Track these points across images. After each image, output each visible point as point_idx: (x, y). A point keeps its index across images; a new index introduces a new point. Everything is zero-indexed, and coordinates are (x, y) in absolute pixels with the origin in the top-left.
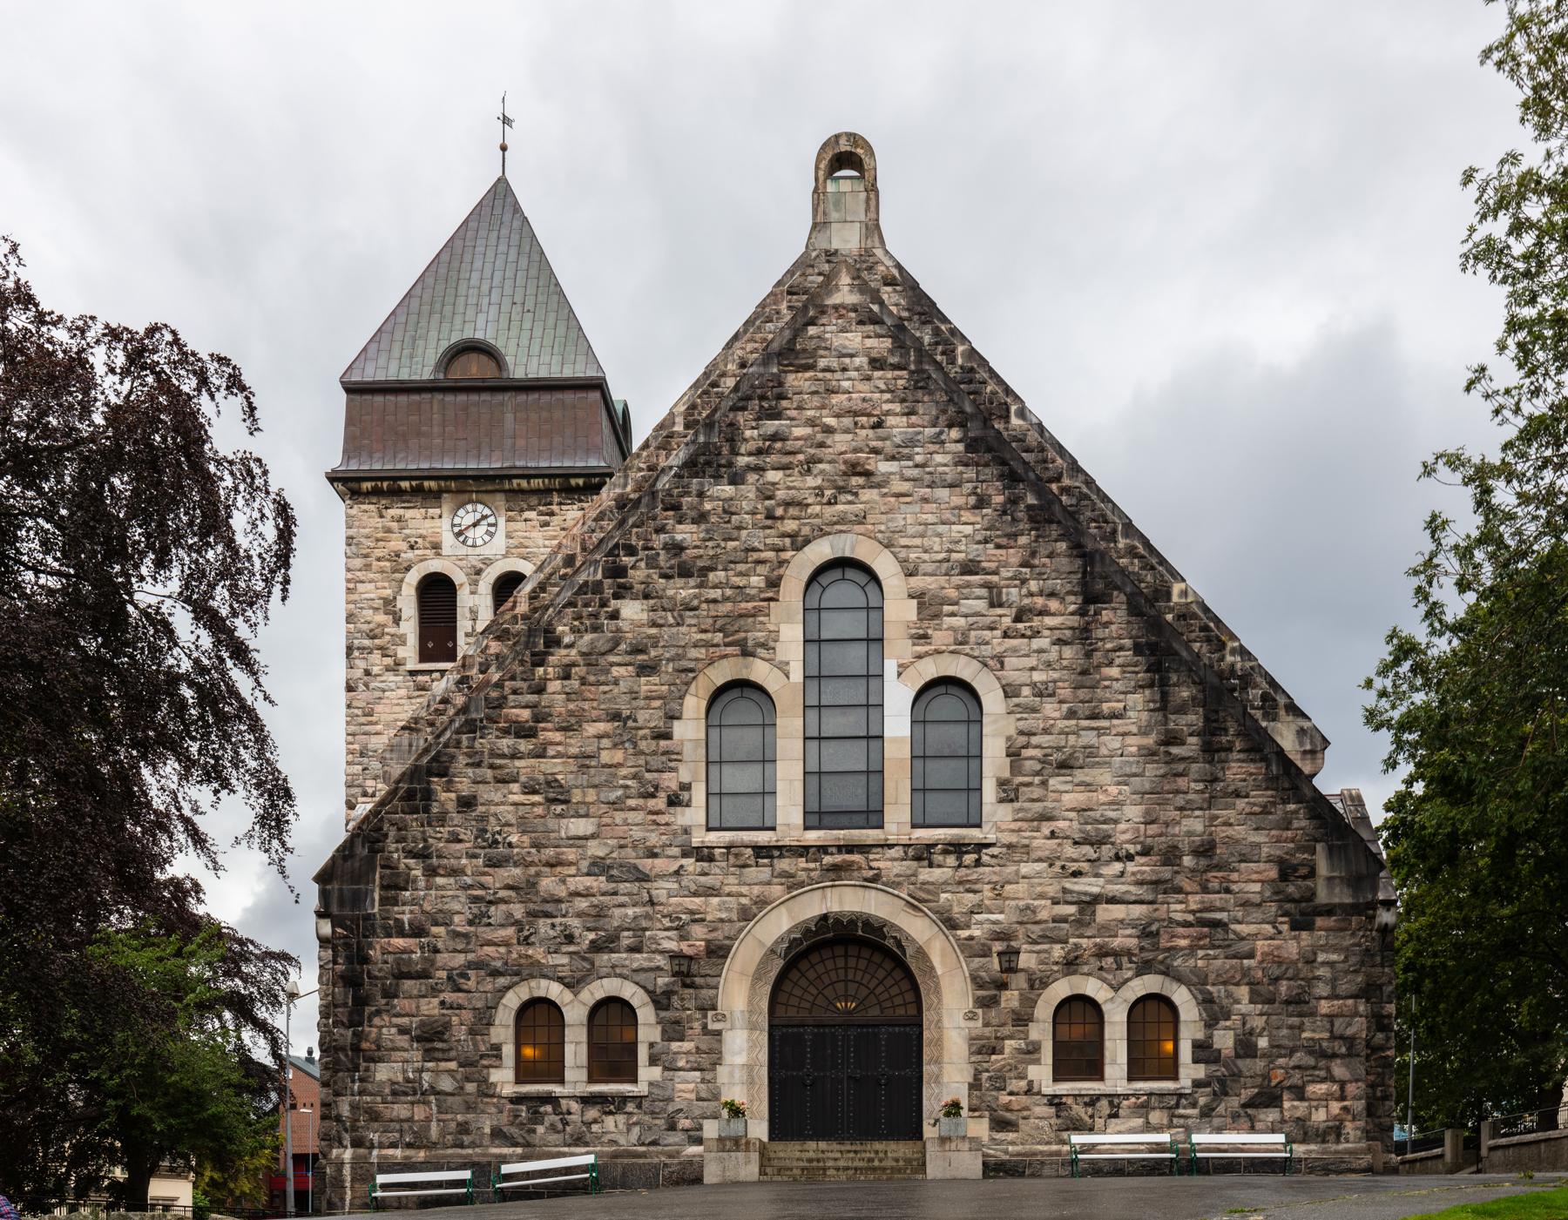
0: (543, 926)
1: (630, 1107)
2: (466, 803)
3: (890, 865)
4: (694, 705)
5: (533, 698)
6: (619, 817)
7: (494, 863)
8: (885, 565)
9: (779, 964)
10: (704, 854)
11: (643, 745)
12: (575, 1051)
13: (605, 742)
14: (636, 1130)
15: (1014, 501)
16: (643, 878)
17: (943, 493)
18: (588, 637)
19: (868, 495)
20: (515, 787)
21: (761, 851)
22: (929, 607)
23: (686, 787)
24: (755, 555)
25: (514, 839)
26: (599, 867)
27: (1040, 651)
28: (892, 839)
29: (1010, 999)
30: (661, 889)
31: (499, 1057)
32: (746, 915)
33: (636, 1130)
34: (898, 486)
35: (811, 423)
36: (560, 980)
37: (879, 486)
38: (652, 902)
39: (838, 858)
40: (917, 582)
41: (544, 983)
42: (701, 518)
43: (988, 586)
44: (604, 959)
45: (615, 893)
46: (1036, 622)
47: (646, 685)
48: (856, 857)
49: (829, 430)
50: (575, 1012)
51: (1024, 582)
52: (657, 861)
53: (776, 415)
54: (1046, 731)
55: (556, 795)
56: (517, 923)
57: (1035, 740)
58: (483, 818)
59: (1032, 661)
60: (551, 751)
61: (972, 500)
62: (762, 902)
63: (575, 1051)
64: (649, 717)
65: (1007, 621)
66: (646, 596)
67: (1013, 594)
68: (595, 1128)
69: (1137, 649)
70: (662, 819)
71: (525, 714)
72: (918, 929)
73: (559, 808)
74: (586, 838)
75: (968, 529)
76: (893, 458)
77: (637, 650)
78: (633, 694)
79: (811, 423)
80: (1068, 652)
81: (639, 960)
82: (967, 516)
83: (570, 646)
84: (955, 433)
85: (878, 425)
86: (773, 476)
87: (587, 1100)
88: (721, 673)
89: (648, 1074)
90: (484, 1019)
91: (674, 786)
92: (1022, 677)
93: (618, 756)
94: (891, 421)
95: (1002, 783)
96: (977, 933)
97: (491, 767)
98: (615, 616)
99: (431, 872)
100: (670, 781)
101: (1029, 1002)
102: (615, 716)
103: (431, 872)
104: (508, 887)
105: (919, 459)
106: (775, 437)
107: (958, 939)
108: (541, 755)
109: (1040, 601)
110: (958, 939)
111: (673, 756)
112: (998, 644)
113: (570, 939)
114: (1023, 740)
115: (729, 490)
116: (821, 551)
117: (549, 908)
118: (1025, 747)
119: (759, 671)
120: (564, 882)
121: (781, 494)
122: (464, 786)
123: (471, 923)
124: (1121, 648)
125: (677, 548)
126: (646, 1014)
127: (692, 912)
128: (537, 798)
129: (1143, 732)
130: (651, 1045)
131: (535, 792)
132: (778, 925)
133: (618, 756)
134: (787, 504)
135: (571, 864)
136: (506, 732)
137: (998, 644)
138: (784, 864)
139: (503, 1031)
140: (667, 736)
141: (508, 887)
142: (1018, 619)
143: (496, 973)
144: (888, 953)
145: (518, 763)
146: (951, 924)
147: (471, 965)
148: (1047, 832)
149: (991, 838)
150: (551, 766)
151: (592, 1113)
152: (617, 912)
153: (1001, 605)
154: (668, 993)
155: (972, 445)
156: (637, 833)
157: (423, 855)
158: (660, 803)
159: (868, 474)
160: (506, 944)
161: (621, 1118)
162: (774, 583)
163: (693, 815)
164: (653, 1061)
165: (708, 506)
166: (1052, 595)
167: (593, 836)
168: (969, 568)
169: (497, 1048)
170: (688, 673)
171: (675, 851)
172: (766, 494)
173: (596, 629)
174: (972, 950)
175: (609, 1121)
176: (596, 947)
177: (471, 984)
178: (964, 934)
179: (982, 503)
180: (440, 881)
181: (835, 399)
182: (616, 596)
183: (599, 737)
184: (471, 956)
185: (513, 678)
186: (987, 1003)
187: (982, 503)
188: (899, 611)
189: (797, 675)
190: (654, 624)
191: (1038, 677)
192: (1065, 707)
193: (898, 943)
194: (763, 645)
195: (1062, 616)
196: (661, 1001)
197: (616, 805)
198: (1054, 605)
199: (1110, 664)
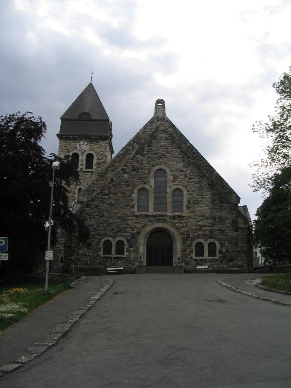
0: (109, 227)
1: (123, 259)
2: (97, 207)
3: (167, 219)
4: (136, 192)
5: (109, 189)
6: (122, 210)
7: (101, 217)
8: (167, 170)
9: (149, 235)
10: (137, 216)
11: (127, 198)
12: (114, 249)
13: (121, 197)
14: (124, 263)
15: (189, 161)
16: (126, 220)
17: (177, 159)
18: (118, 180)
19: (165, 159)
20: (105, 204)
21: (147, 216)
22: (175, 177)
23: (134, 205)
24: (146, 168)
25: (104, 213)
26: (118, 218)
27: (193, 185)
28: (168, 215)
29: (188, 242)
30: (129, 222)
31: (100, 250)
32: (143, 227)
33: (124, 263)
34: (170, 158)
35: (156, 147)
36: (111, 237)
37: (166, 157)
38: (127, 224)
39: (159, 218)
40: (173, 173)
41: (109, 237)
42: (138, 161)
43: (184, 174)
44: (119, 234)
45: (121, 222)
46: (192, 180)
47: (128, 188)
48: (162, 218)
49: (159, 149)
50: (114, 243)
51: (190, 173)
52: (129, 217)
53: (150, 146)
54: (194, 198)
55: (112, 205)
56: (105, 227)
57: (192, 199)
58: (100, 209)
59: (192, 186)
60: (111, 199)
61: (182, 160)
62: (146, 225)
63: (114, 249)
64: (128, 193)
65: (187, 180)
66: (128, 174)
67: (188, 175)
68: (116, 263)
69: (209, 185)
70: (130, 210)
71: (107, 192)
72: (173, 230)
73: (112, 208)
74: (116, 213)
75: (181, 165)
76: (169, 153)
77: (126, 182)
78: (125, 189)
79: (156, 147)
80: (198, 185)
81: (125, 234)
82: (181, 163)
83: (116, 181)
84: (179, 150)
85: (167, 148)
86: (149, 155)
87: (115, 258)
88: (140, 187)
89: (126, 254)
90: (98, 243)
91: (132, 205)
92: (190, 189)
93: (123, 200)
94: (169, 148)
95: (187, 206)
96: (182, 231)
97: (101, 200)
98: (123, 176)
99: (90, 218)
100: (131, 204)
101: (191, 243)
102: (122, 193)
103: (90, 218)
104: (103, 221)
105: (173, 154)
106: (150, 149)
107: (179, 232)
108: (109, 199)
109: (193, 177)
110: (179, 232)
111: (132, 200)
112: (186, 183)
113: (113, 230)
114: (190, 199)
115: (142, 157)
116: (157, 167)
117: (110, 225)
118: (191, 200)
119: (147, 186)
120: (112, 220)
121: (151, 158)
122: (96, 203)
123: (97, 227)
124: (206, 185)
125: (133, 166)
126: (126, 243)
127: (134, 226)
128: (109, 206)
129: (210, 198)
130: (127, 249)
131: (108, 205)
132: (149, 229)
133: (123, 200)
134: (152, 160)
135: (114, 217)
136: (104, 195)
137: (186, 183)
138: (150, 218)
139: (101, 246)
140: (131, 196)
141: (103, 221)
142: (189, 179)
143: (100, 235)
144: (167, 234)
145: (106, 200)
146: (178, 229)
147: (96, 234)
148: (194, 214)
149: (185, 215)
150: (112, 201)
151: (116, 260)
152: (122, 226)
153: (186, 177)
154: (130, 240)
155: (182, 152)
156: (125, 212)
157: (89, 215)
158: (129, 207)
159: (165, 156)
160: (102, 230)
161: (121, 261)
162: (149, 172)
163: (135, 210)
164: (127, 251)
165: (139, 160)
166: (195, 176)
167: (118, 213)
168: (181, 171)
169: (100, 248)
170: (135, 186)
171: (132, 216)
172: (148, 158)
173: (120, 178)
174: (182, 234)
175: (119, 262)
176: (118, 231)
177: (96, 237)
178: (180, 231)
179: (183, 161)
180: (92, 219)
181: (160, 144)
182: (123, 174)
183: (120, 196)
184: (96, 232)
185: (106, 186)
186: (184, 243)
187: (183, 161)
188: (170, 177)
189: (153, 187)
190: (129, 178)
191: (192, 189)
192: (197, 194)
193: (169, 232)
194: (147, 182)
195: (196, 180)
196: (128, 241)
197: (122, 208)
198: (195, 177)
199: (204, 187)
